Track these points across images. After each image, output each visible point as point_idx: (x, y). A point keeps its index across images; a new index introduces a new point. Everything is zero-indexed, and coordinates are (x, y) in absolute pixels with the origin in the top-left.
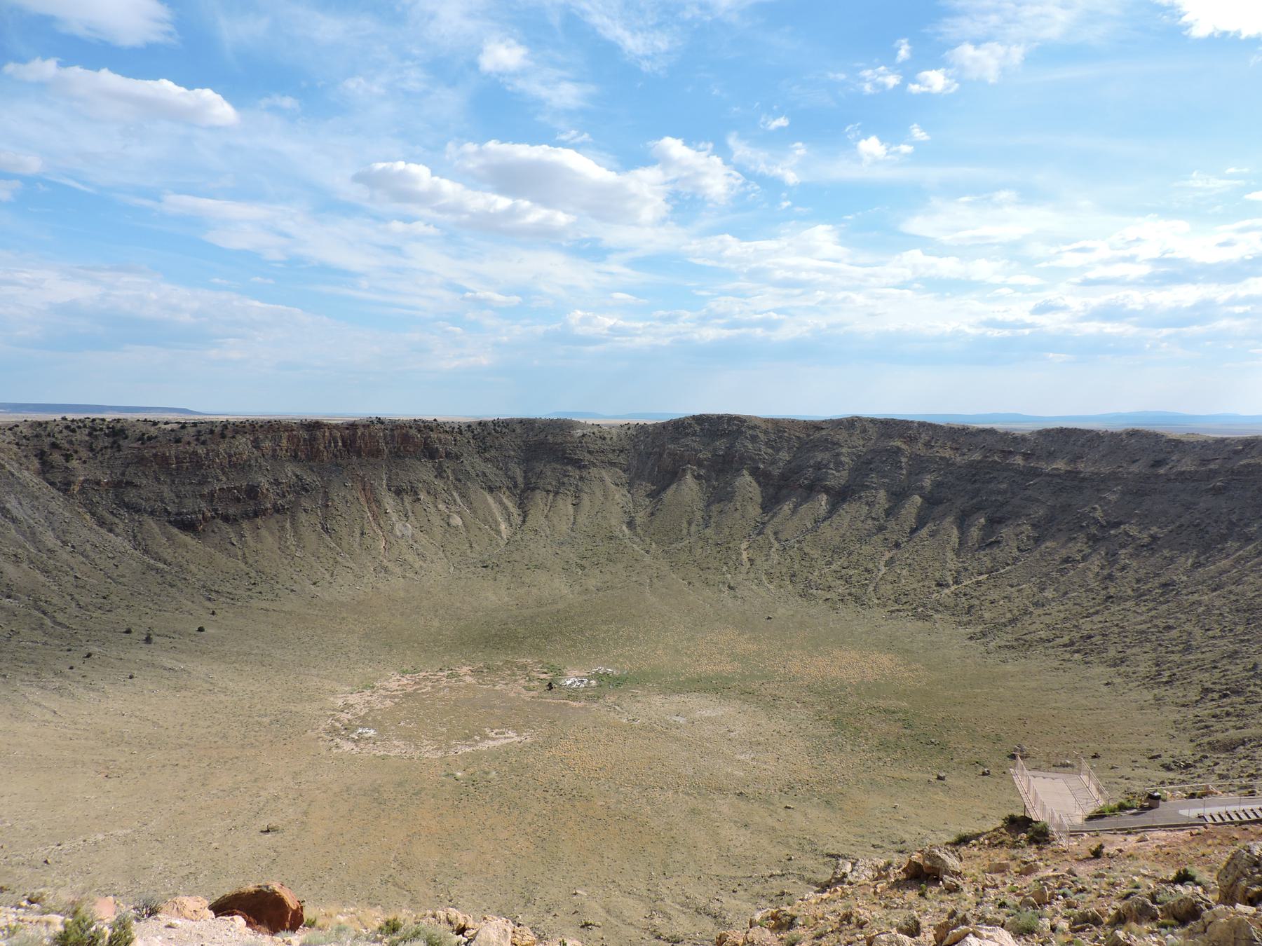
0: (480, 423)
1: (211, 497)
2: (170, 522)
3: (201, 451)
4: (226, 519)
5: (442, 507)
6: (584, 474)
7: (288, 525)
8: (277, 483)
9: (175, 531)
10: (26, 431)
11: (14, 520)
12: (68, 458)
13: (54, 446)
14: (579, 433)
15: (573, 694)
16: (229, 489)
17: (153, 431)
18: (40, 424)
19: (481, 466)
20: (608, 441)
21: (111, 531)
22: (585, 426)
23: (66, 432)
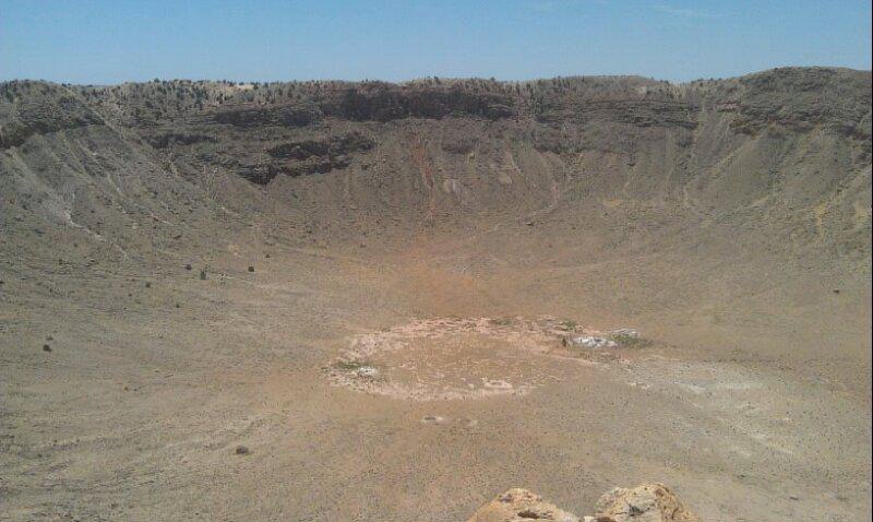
0: (540, 82)
1: (274, 153)
2: (241, 174)
3: (269, 106)
4: (285, 170)
5: (493, 166)
6: (646, 132)
7: (346, 180)
8: (337, 139)
9: (244, 182)
10: (127, 92)
11: (109, 168)
12: (158, 115)
13: (149, 105)
14: (643, 90)
15: (585, 352)
16: (293, 145)
17: (229, 91)
18: (137, 86)
19: (534, 124)
20: (676, 95)
21: (188, 180)
22: (651, 82)
23: (157, 93)
